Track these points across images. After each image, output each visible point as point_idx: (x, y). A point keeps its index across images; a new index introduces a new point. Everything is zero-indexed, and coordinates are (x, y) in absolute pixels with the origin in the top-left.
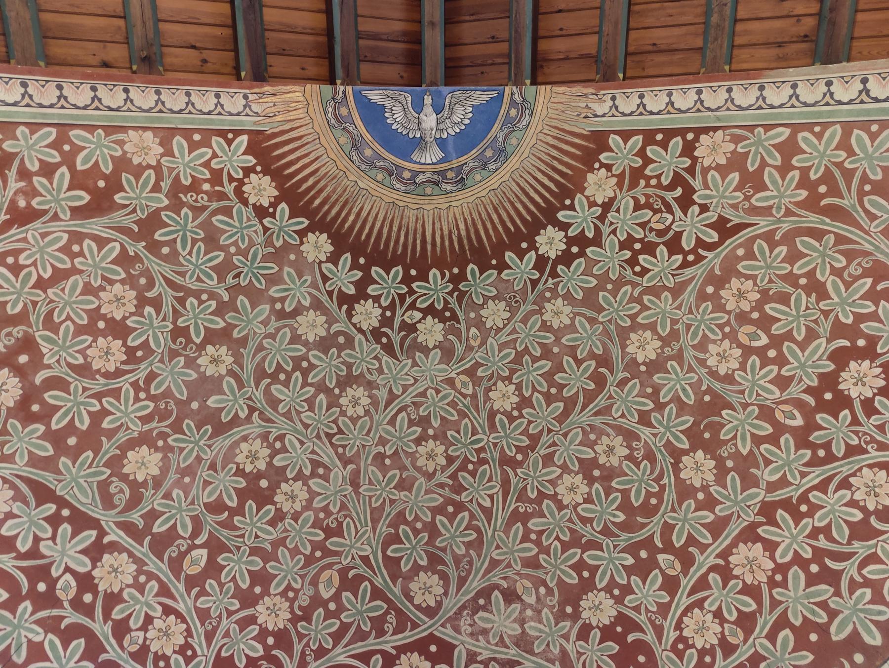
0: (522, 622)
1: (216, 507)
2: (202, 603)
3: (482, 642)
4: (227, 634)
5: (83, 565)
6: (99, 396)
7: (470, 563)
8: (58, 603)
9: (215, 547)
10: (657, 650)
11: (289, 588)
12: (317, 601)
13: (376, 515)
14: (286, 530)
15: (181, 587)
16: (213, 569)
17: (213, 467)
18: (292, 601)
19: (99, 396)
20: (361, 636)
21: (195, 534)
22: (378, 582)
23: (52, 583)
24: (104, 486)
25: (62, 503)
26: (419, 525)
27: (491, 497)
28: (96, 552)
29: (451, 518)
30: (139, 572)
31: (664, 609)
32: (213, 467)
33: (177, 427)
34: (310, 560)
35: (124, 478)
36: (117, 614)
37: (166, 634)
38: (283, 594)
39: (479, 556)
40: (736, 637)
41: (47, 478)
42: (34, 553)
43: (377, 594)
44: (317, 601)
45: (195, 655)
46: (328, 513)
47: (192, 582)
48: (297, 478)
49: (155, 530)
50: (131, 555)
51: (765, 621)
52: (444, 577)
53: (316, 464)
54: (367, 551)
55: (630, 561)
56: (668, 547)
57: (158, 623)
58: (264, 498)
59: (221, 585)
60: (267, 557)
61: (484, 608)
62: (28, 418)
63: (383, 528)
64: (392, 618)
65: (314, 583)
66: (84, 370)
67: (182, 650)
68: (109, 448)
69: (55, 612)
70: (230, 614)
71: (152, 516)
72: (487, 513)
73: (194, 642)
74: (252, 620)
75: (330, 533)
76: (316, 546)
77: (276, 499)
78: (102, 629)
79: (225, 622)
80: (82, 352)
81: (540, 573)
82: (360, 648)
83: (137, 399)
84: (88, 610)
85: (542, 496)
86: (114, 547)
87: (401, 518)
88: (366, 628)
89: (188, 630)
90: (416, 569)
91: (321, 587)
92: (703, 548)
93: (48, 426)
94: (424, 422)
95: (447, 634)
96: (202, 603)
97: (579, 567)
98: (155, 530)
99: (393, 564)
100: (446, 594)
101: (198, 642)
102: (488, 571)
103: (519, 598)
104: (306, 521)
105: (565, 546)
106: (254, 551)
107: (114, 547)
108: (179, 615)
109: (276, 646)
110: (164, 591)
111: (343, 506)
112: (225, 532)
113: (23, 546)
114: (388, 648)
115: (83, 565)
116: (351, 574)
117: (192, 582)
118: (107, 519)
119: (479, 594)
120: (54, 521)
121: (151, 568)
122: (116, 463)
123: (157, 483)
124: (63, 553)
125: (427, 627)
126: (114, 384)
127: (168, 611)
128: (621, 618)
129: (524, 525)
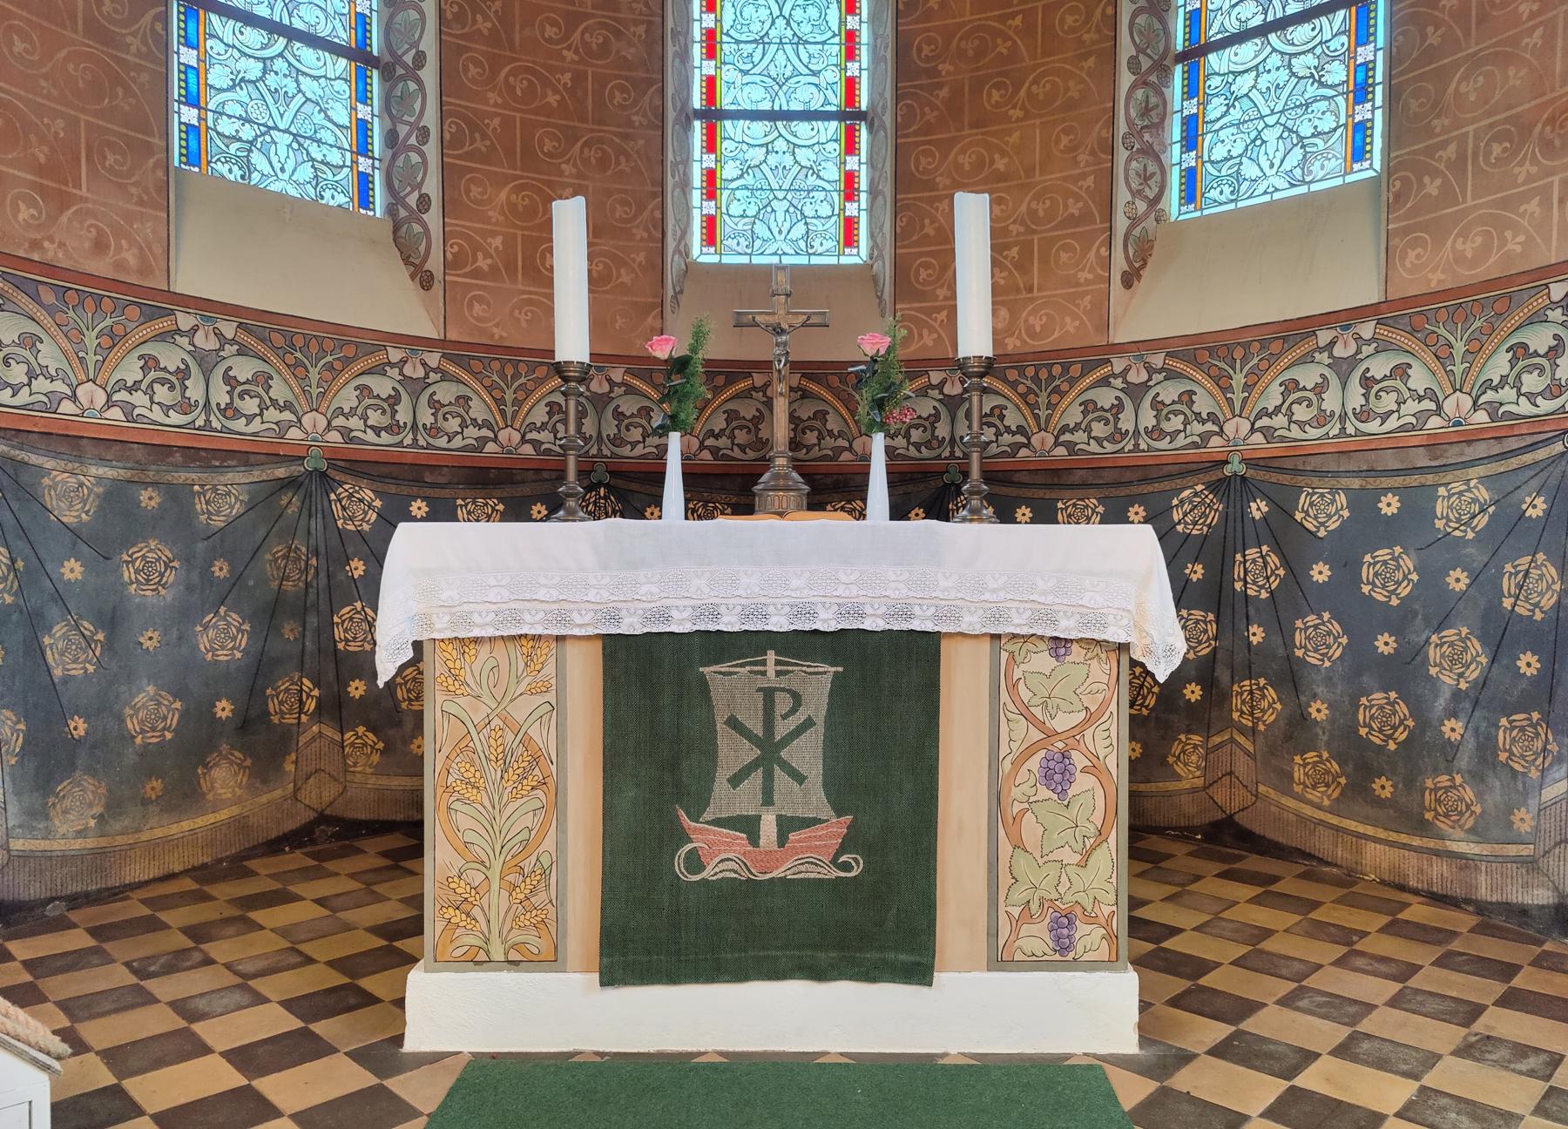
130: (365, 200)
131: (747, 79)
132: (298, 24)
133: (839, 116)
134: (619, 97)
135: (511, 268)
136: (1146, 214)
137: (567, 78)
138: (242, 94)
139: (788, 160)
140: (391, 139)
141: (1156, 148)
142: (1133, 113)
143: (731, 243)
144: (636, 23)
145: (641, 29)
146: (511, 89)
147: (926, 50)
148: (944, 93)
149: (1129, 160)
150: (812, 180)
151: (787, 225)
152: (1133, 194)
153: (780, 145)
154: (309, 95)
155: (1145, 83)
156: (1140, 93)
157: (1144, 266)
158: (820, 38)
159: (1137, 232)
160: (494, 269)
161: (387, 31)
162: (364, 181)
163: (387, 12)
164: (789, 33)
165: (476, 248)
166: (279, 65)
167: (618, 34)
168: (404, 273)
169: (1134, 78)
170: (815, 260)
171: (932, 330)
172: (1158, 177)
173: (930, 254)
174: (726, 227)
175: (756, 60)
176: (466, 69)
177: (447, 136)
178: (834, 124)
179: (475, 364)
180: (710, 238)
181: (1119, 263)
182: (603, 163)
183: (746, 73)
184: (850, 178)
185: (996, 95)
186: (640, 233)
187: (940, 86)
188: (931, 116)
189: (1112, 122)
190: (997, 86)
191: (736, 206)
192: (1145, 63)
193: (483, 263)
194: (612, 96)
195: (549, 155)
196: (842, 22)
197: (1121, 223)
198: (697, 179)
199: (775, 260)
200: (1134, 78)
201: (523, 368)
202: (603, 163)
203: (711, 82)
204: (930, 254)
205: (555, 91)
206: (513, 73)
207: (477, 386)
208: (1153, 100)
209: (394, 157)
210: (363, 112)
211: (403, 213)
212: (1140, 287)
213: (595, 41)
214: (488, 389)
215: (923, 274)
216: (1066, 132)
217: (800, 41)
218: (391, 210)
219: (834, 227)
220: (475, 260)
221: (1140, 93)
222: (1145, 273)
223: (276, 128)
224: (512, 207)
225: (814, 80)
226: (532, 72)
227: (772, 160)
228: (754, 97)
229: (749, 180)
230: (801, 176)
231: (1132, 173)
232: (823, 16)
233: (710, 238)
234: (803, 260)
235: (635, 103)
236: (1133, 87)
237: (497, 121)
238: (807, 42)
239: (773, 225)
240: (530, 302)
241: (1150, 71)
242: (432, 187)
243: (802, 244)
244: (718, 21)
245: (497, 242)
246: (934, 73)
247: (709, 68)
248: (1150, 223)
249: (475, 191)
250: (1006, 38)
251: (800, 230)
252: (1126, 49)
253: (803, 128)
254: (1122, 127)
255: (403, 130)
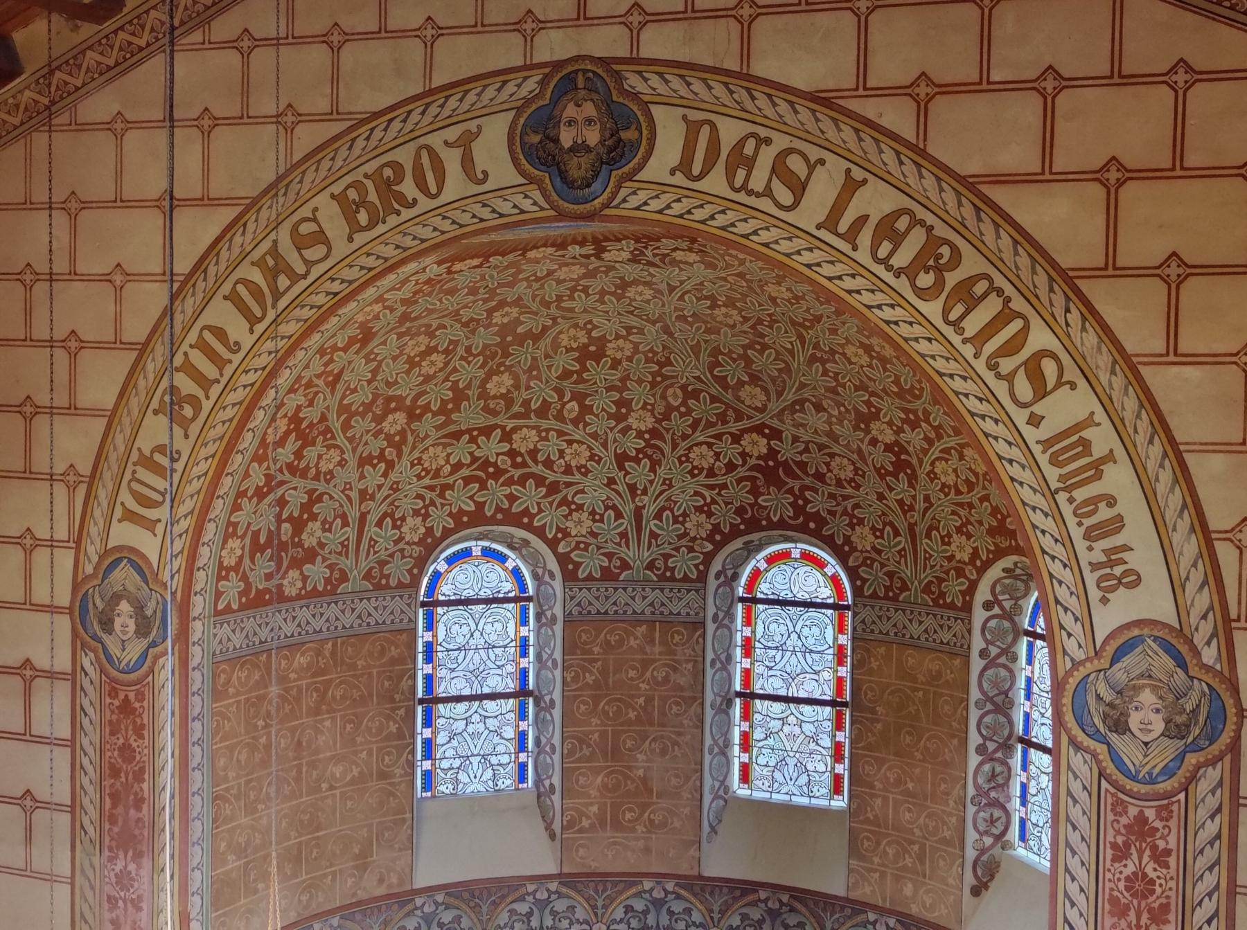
0: (830, 424)
1: (566, 375)
2: (589, 430)
3: (802, 430)
4: (615, 441)
5: (506, 447)
6: (446, 379)
7: (784, 381)
8: (507, 471)
9: (579, 397)
10: (919, 472)
11: (646, 404)
12: (670, 409)
13: (696, 350)
14: (626, 370)
15: (570, 427)
16: (585, 410)
17: (547, 356)
18: (652, 411)
19: (446, 379)
20: (710, 425)
21: (561, 396)
22: (713, 391)
23: (495, 465)
24: (486, 409)
25: (469, 431)
26: (734, 356)
27: (791, 343)
28: (507, 437)
29: (761, 352)
30: (539, 432)
31: (925, 452)
32: (547, 356)
33: (506, 355)
34: (654, 385)
35: (495, 397)
36: (540, 457)
37: (577, 454)
38: (644, 408)
39: (790, 378)
40: (964, 489)
41: (452, 428)
42: (475, 459)
43: (714, 399)
44: (670, 409)
45: (601, 458)
46: (656, 353)
47: (575, 422)
48: (618, 337)
49: (533, 408)
50: (527, 427)
51: (978, 492)
52: (764, 389)
53: (629, 329)
54: (698, 373)
55: (903, 416)
56: (927, 421)
57: (568, 451)
58: (598, 356)
59: (597, 416)
60: (620, 390)
61: (800, 411)
62: (419, 418)
63: (705, 357)
64: (730, 413)
65: (664, 397)
66: (428, 379)
67: (591, 458)
68: (473, 393)
69: (507, 475)
70: (611, 429)
71: (526, 403)
72: (791, 352)
73: (596, 451)
74: (629, 428)
75: (661, 365)
76: (654, 375)
77: (608, 353)
78: (539, 469)
79: (610, 435)
80: (419, 375)
81: (839, 398)
82: (712, 431)
83: (469, 363)
84: (524, 464)
85: (833, 352)
86: (515, 430)
87: (716, 352)
88: (714, 419)
89: (589, 446)
90: (741, 383)
91: (670, 399)
92: (949, 436)
93: (431, 411)
94: (712, 298)
95: (775, 423)
96: (589, 430)
97: (868, 403)
98: (533, 408)
99: (722, 380)
100: (769, 400)
101: (599, 450)
102: (798, 389)
103: (825, 410)
104: (639, 361)
105: (857, 389)
106: (608, 389)
107: (515, 430)
108: (578, 442)
109: (652, 438)
110: (561, 433)
111: (664, 347)
112: (580, 386)
113: (467, 460)
114: (733, 430)
115: (506, 447)
116: (690, 388)
117: (575, 422)
118: (499, 420)
119: (795, 402)
120: (473, 440)
121: (545, 426)
122: (483, 395)
123: (517, 386)
124: (490, 449)
125: (758, 419)
126: (450, 368)
127: (570, 443)
128: (897, 443)
129: (823, 366)
130: (522, 778)
131: (771, 673)
132: (486, 690)
133: (831, 703)
134: (675, 709)
135: (602, 823)
136: (993, 846)
137: (642, 700)
138: (454, 743)
139: (797, 730)
140: (537, 742)
141: (1001, 800)
142: (980, 781)
143: (759, 783)
144: (688, 661)
145: (690, 666)
146: (606, 713)
147: (870, 695)
148: (879, 726)
149: (977, 812)
150: (812, 746)
151: (796, 775)
152: (981, 834)
153: (792, 719)
154: (492, 728)
155: (992, 759)
156: (987, 767)
157: (992, 877)
158: (820, 649)
159: (984, 858)
160: (592, 826)
161: (538, 676)
162: (523, 767)
163: (537, 665)
164: (800, 644)
165: (582, 814)
166: (476, 718)
167: (675, 669)
168: (542, 826)
169: (980, 758)
170: (814, 801)
171: (870, 884)
172: (1004, 819)
173: (870, 831)
174: (757, 771)
175: (777, 660)
176: (578, 708)
177: (566, 752)
178: (828, 709)
179: (580, 886)
180: (745, 777)
181: (969, 879)
182: (664, 752)
183: (771, 668)
184: (838, 747)
185: (908, 739)
186: (686, 795)
187: (878, 721)
188: (872, 739)
189: (965, 786)
190: (909, 733)
191: (763, 760)
192: (991, 746)
193: (586, 823)
194: (671, 709)
195: (629, 750)
196: (835, 639)
197: (971, 854)
198: (737, 740)
199: (787, 798)
200: (980, 758)
201: (609, 885)
202: (664, 752)
203: (747, 674)
204: (870, 831)
205: (634, 709)
206: (607, 703)
207: (581, 899)
208: (998, 769)
209: (539, 753)
210: (523, 725)
211: (542, 789)
212: (987, 896)
213: (660, 675)
214: (587, 900)
215: (866, 844)
216: (944, 780)
217: (807, 651)
218: (538, 782)
219: (827, 779)
220: (581, 821)
221: (987, 767)
222: (992, 885)
223: (473, 755)
224: (605, 786)
225: (816, 677)
226: (619, 700)
227: (786, 729)
228: (775, 685)
229: (771, 741)
230: (806, 742)
231: (980, 821)
232: (823, 633)
233: (745, 777)
234: (804, 801)
235: (685, 711)
236: (981, 764)
237: (596, 735)
238: (811, 651)
239: (786, 774)
240: (615, 843)
241: (995, 751)
242: (556, 780)
243: (805, 789)
244: (753, 632)
245: (595, 809)
246: (874, 711)
247: (746, 663)
248: (997, 850)
249: (582, 780)
250: (914, 703)
251: (804, 779)
252: (974, 739)
253: (807, 709)
254: (971, 791)
255: (544, 740)
